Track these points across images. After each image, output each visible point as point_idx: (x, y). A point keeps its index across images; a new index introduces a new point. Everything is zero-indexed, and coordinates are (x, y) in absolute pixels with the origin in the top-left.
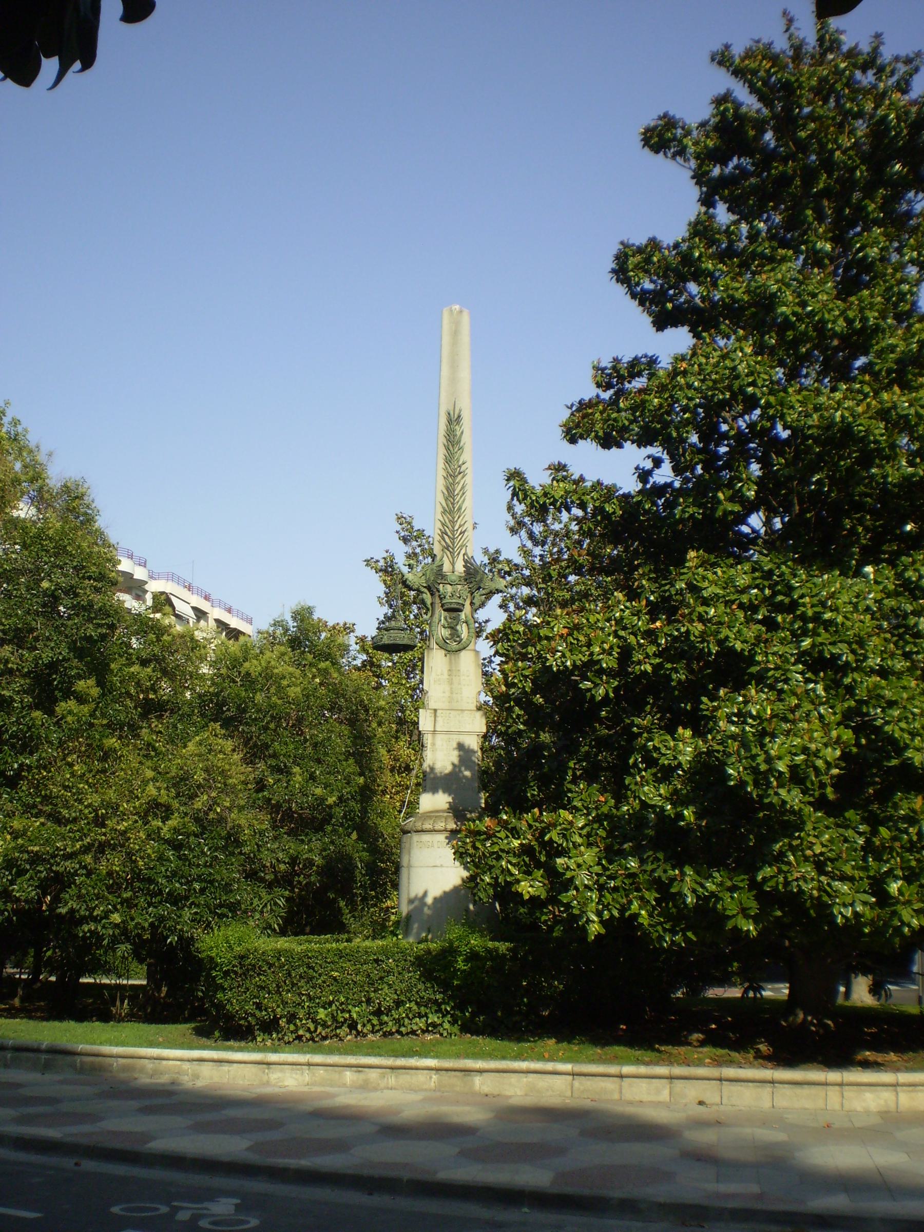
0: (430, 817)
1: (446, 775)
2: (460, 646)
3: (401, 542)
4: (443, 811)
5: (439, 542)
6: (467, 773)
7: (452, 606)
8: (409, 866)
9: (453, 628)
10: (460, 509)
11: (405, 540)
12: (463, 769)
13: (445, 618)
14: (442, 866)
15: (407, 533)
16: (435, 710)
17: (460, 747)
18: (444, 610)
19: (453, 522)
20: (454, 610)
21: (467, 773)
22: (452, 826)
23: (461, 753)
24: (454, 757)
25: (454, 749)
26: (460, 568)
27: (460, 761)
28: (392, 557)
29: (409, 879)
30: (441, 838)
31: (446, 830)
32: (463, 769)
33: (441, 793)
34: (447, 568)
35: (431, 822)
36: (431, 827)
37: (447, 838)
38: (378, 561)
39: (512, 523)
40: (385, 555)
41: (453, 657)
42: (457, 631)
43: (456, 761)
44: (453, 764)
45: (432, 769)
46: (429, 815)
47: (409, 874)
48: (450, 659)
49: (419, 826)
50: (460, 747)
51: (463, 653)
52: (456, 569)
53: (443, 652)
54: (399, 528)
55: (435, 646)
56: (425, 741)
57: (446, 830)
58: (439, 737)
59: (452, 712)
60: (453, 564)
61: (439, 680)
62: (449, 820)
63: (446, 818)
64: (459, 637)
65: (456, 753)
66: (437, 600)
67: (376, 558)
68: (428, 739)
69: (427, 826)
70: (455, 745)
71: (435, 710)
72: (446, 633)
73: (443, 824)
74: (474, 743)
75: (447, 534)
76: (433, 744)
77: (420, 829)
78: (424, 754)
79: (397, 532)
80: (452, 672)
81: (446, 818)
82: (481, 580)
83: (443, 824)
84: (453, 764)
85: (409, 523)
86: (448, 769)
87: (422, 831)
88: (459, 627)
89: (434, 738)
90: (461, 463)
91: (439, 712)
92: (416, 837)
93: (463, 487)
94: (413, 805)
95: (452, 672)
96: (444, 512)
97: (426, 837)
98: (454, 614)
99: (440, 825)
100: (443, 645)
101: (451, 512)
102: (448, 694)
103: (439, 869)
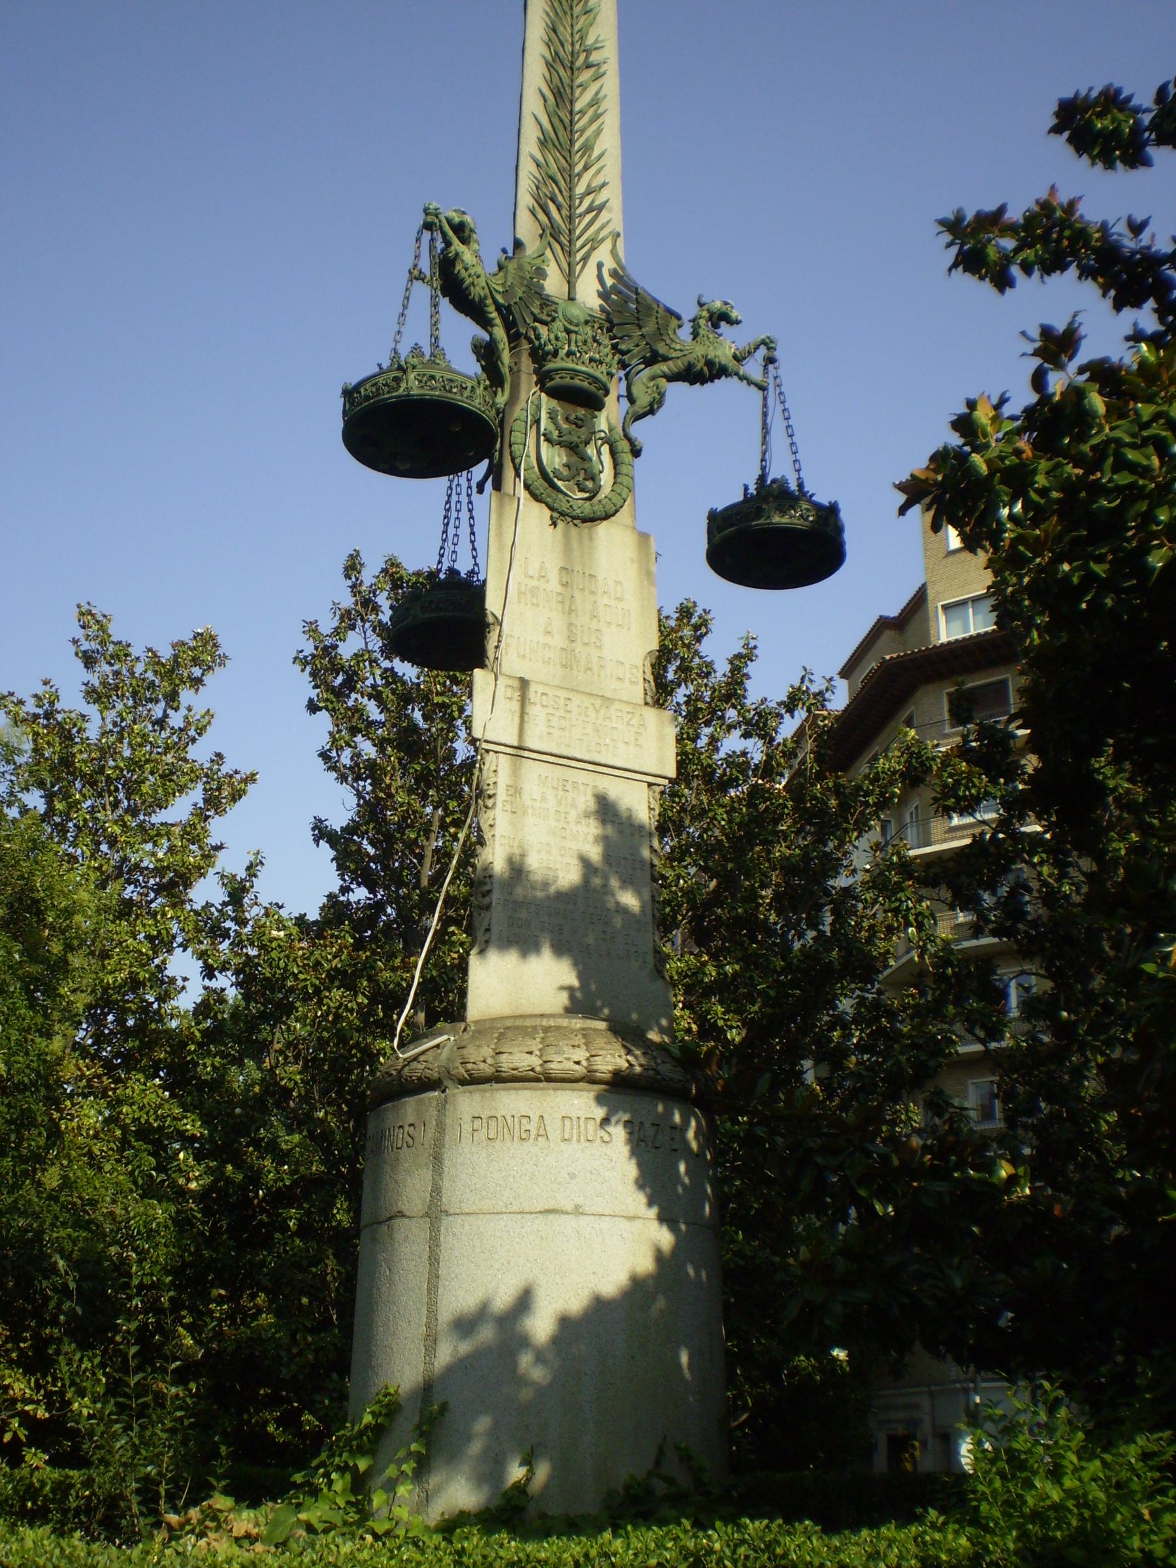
0: (527, 1032)
1: (561, 896)
2: (599, 510)
3: (79, 664)
4: (560, 1016)
5: (533, 213)
6: (629, 900)
7: (577, 382)
8: (435, 1213)
9: (574, 449)
10: (587, 148)
11: (89, 660)
12: (614, 882)
13: (552, 416)
14: (578, 1211)
15: (94, 645)
16: (524, 684)
17: (605, 810)
18: (554, 393)
19: (572, 179)
20: (583, 399)
21: (629, 900)
22: (613, 1058)
23: (610, 830)
24: (586, 839)
25: (587, 816)
26: (589, 295)
27: (607, 856)
28: (54, 698)
29: (434, 1260)
30: (582, 1104)
31: (589, 1078)
32: (614, 882)
33: (547, 953)
34: (553, 284)
35: (535, 1046)
36: (535, 1061)
37: (600, 1100)
38: (21, 702)
39: (348, 601)
40: (40, 690)
41: (574, 531)
42: (585, 458)
43: (595, 853)
44: (585, 862)
45: (517, 870)
46: (508, 1029)
47: (434, 1243)
48: (566, 535)
49: (481, 1056)
50: (605, 810)
51: (603, 528)
52: (579, 296)
53: (548, 513)
54: (80, 633)
55: (522, 492)
56: (488, 777)
57: (589, 1078)
58: (534, 773)
59: (577, 699)
60: (571, 279)
61: (534, 591)
62: (600, 1041)
63: (585, 1033)
64: (593, 478)
65: (593, 828)
66: (527, 365)
67: (19, 695)
68: (497, 772)
69: (519, 1059)
70: (587, 801)
71: (524, 684)
72: (554, 458)
73: (581, 1054)
74: (641, 805)
75: (553, 200)
76: (515, 790)
77: (487, 1069)
78: (485, 819)
79: (75, 642)
80: (574, 575)
81: (585, 1033)
82: (660, 333)
83: (581, 1054)
84: (585, 862)
85: (103, 628)
86: (568, 876)
87: (498, 1078)
88: (591, 451)
89: (515, 772)
90: (590, 41)
91: (533, 688)
92: (467, 1104)
93: (595, 102)
94: (445, 999)
95: (574, 575)
96: (543, 143)
97: (513, 1102)
98: (581, 412)
99: (569, 1057)
100: (544, 488)
101: (558, 146)
102: (558, 641)
103: (568, 1224)
